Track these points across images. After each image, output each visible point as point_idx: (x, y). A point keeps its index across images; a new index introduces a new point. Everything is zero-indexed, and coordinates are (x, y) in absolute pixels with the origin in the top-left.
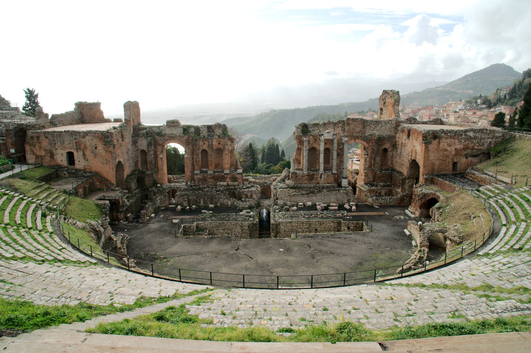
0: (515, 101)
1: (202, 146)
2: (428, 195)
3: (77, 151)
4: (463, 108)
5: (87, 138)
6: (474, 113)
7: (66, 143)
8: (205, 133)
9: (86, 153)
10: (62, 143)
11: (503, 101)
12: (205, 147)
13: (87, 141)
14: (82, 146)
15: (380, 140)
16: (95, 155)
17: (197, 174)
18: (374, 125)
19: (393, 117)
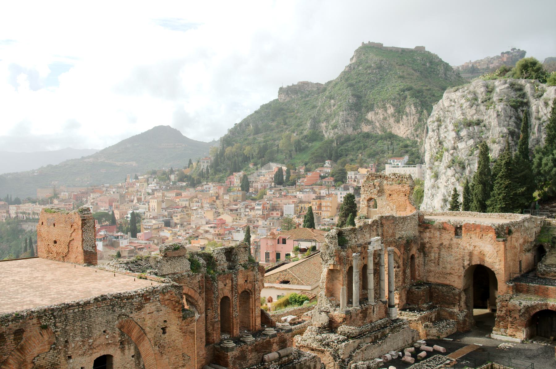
0: (221, 175)
1: (222, 289)
2: (533, 307)
3: (123, 349)
4: (158, 187)
5: (149, 307)
6: (179, 195)
7: (97, 333)
8: (223, 263)
9: (141, 349)
10: (87, 334)
11: (206, 176)
12: (227, 292)
13: (148, 317)
14: (135, 333)
15: (408, 244)
16: (161, 348)
17: (232, 349)
18: (402, 223)
19: (414, 212)
